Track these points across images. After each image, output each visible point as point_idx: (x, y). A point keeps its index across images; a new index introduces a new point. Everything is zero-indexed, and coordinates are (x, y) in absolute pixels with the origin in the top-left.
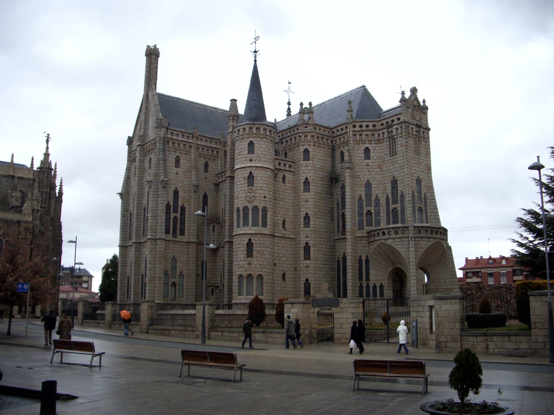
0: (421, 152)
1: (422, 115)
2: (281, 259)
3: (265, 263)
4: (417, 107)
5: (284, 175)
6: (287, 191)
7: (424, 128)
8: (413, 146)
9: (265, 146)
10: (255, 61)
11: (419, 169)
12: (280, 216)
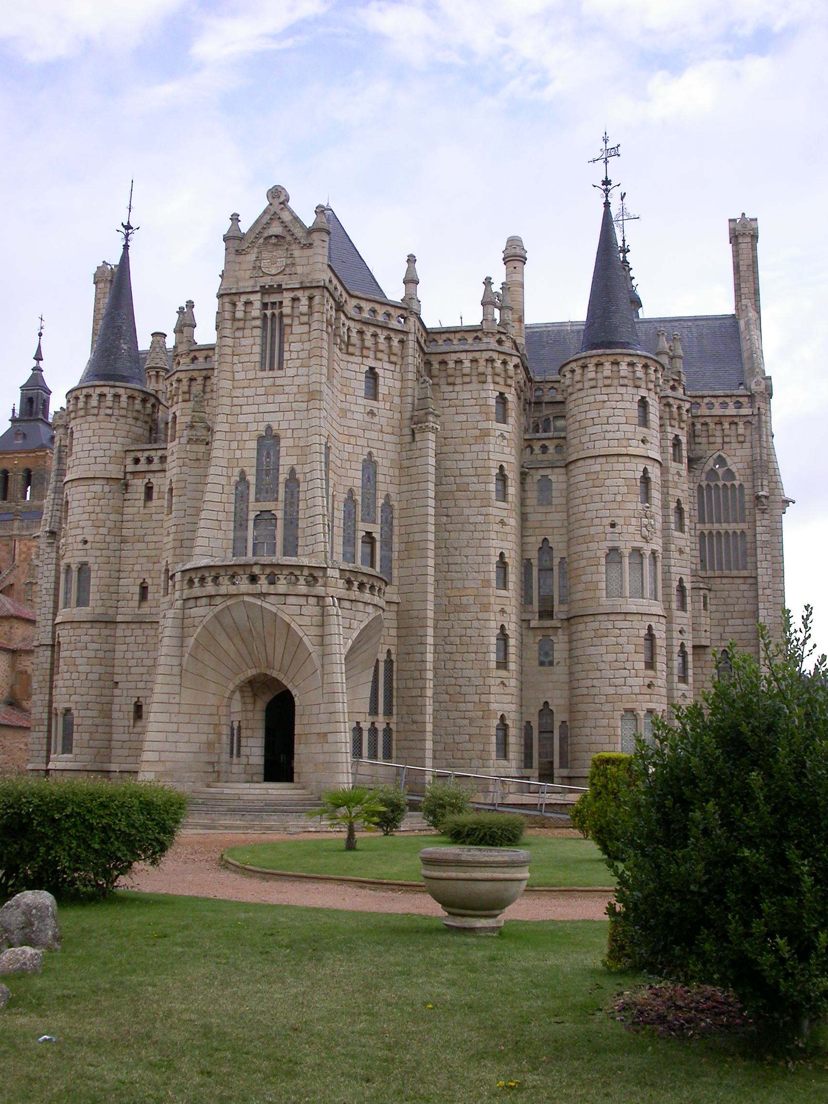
0: (286, 356)
1: (297, 253)
2: (133, 670)
3: (77, 683)
4: (273, 240)
5: (149, 482)
6: (155, 517)
7: (293, 290)
8: (257, 349)
9: (90, 433)
10: (126, 247)
11: (271, 407)
12: (135, 575)
